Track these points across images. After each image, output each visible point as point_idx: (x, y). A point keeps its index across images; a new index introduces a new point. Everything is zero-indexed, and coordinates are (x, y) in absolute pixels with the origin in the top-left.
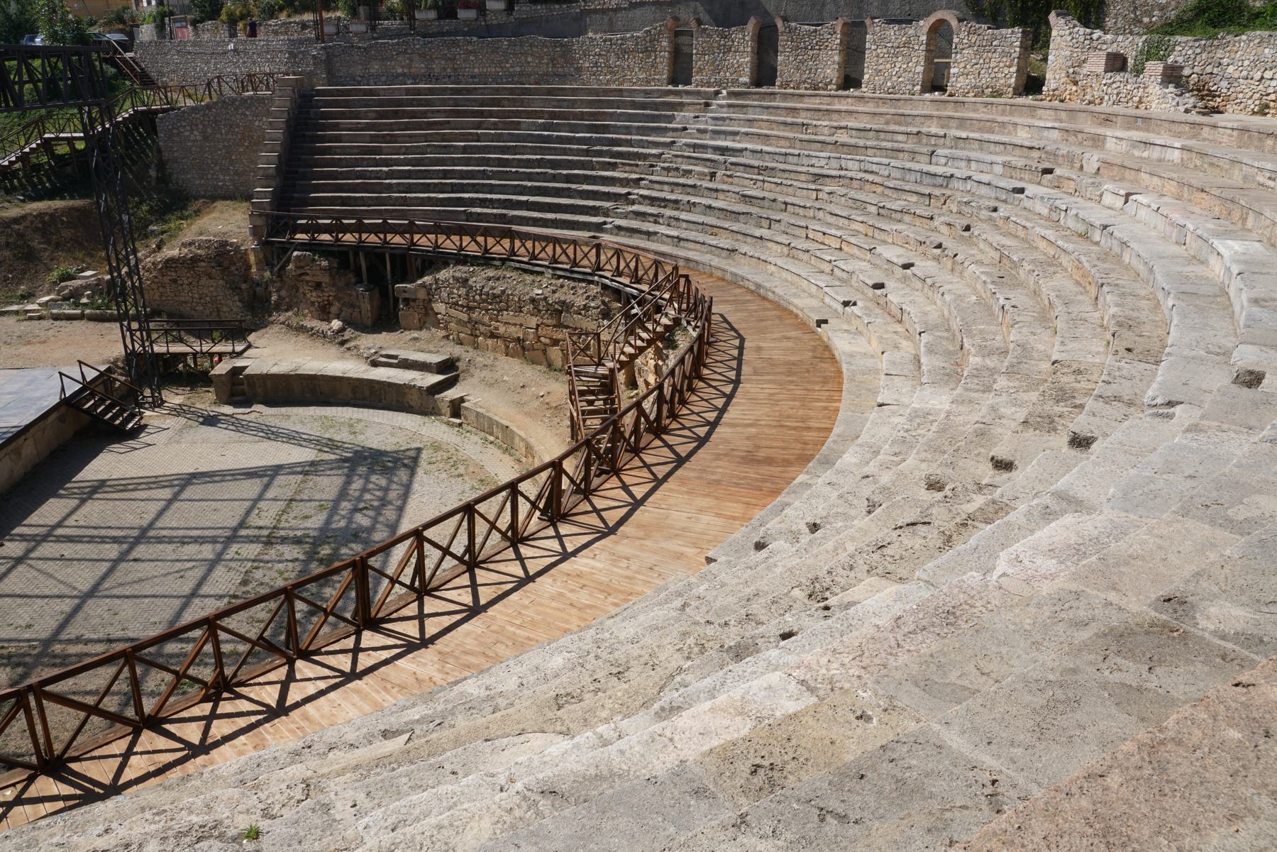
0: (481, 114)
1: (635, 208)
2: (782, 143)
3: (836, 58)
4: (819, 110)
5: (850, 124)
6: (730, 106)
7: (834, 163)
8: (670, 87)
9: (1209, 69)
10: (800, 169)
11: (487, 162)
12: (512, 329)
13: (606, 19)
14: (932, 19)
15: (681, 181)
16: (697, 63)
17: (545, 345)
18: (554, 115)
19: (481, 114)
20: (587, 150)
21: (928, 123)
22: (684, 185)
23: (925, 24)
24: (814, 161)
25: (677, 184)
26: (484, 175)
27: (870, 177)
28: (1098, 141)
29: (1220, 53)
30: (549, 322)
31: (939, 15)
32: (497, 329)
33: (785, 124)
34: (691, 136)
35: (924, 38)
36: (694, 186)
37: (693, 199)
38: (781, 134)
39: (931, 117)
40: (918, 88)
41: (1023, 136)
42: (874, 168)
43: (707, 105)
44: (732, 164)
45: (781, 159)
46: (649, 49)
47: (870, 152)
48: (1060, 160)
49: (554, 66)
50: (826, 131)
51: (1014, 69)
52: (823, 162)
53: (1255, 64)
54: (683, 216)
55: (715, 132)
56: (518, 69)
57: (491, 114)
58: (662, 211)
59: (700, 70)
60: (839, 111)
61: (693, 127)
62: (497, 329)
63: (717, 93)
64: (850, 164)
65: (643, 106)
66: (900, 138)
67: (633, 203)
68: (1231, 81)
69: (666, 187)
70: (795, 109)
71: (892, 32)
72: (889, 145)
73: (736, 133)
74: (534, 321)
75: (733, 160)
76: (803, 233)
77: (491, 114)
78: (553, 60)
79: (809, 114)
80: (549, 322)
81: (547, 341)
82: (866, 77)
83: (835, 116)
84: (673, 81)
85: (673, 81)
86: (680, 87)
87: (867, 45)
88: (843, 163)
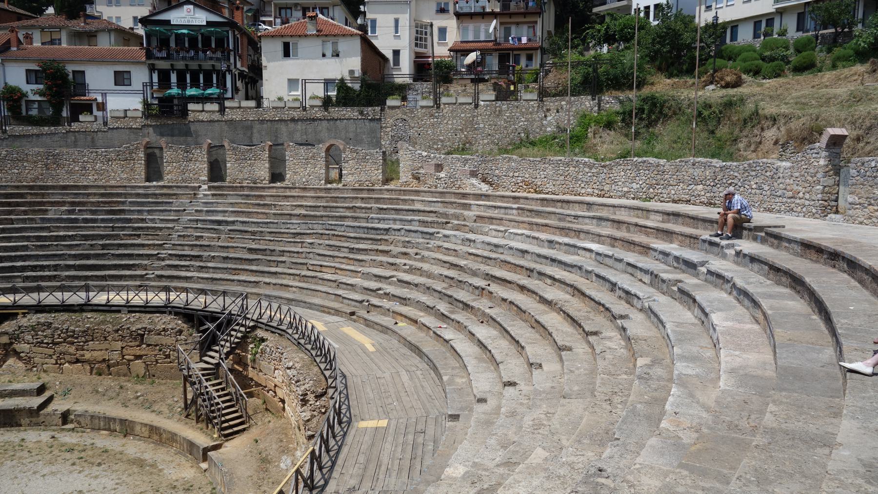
0: (9, 204)
1: (168, 262)
2: (261, 216)
3: (267, 165)
4: (279, 196)
5: (305, 204)
6: (213, 195)
7: (304, 226)
8: (147, 184)
9: (486, 172)
10: (282, 231)
11: (28, 239)
12: (96, 354)
13: (89, 138)
14: (327, 145)
15: (198, 243)
16: (167, 168)
17: (129, 361)
18: (73, 204)
19: (9, 204)
20: (112, 227)
21: (355, 201)
22: (201, 246)
23: (323, 147)
24: (289, 226)
25: (196, 245)
26: (25, 248)
27: (333, 232)
28: (467, 207)
29: (490, 164)
30: (132, 344)
31: (332, 142)
32: (83, 355)
33: (259, 205)
34: (190, 214)
35: (324, 154)
36: (209, 246)
37: (213, 254)
38: (259, 211)
39: (357, 198)
40: (323, 182)
41: (418, 206)
42: (333, 227)
43: (195, 194)
44: (230, 230)
45: (264, 226)
46: (129, 159)
47: (324, 219)
48: (450, 217)
49: (48, 169)
50: (289, 208)
51: (380, 171)
52: (296, 226)
53: (508, 170)
54: (210, 265)
55: (207, 211)
56: (16, 171)
57: (18, 204)
58: (192, 263)
59: (170, 172)
60: (293, 197)
61: (191, 209)
62: (83, 355)
63: (200, 187)
64: (315, 226)
65: (146, 196)
66: (341, 210)
67: (163, 259)
68: (498, 177)
69: (186, 248)
70: (261, 196)
71: (302, 150)
72: (337, 214)
73: (226, 212)
74: (120, 344)
75: (229, 228)
76: (305, 267)
77: (18, 204)
78: (46, 165)
79: (272, 199)
80: (132, 344)
81: (132, 358)
82: (288, 176)
83: (291, 199)
84: (148, 179)
85: (148, 179)
86: (155, 183)
87: (287, 158)
88: (310, 226)
